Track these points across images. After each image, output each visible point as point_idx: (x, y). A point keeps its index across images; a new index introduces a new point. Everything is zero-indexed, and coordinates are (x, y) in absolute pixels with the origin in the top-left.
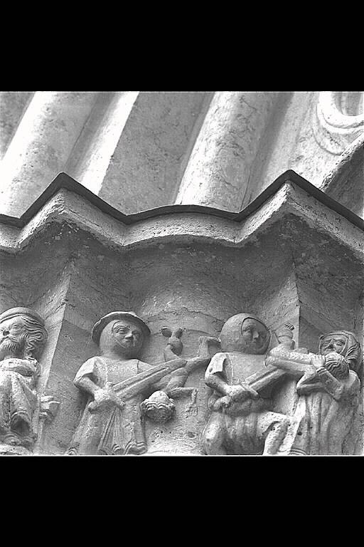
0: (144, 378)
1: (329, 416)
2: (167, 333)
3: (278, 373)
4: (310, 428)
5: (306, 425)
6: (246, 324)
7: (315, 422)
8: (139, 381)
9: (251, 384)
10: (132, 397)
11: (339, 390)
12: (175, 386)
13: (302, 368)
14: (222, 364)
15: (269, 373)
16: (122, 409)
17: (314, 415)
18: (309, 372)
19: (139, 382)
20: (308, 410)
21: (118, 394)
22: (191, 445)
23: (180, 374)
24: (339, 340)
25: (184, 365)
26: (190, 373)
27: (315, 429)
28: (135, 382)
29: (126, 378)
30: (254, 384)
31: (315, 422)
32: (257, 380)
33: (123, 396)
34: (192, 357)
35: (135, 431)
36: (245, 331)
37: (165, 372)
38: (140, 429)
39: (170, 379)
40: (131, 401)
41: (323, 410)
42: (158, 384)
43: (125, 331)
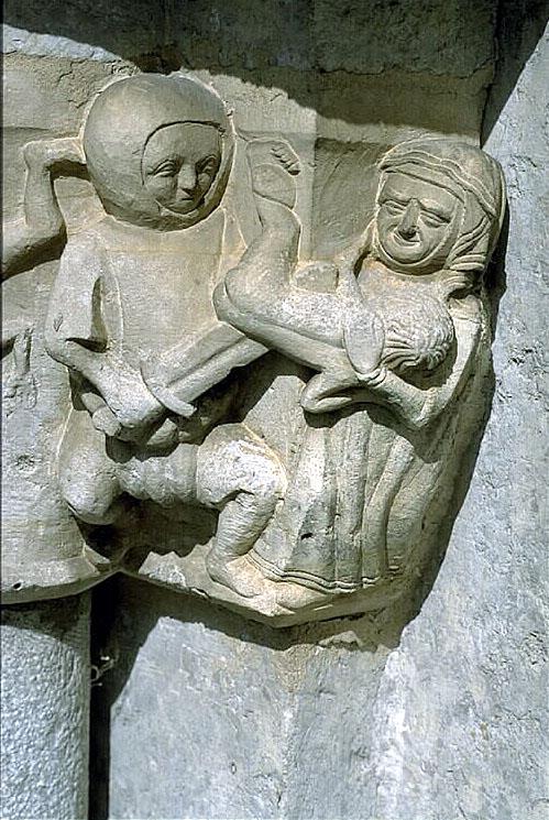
1: (389, 477)
3: (249, 351)
4: (333, 513)
5: (324, 516)
6: (157, 152)
7: (348, 505)
9: (173, 382)
11: (420, 417)
13: (312, 353)
14: (87, 300)
15: (221, 351)
17: (345, 483)
18: (336, 371)
20: (330, 472)
24: (431, 210)
27: (347, 522)
30: (183, 384)
31: (348, 505)
32: (191, 371)
36: (155, 172)
41: (370, 469)
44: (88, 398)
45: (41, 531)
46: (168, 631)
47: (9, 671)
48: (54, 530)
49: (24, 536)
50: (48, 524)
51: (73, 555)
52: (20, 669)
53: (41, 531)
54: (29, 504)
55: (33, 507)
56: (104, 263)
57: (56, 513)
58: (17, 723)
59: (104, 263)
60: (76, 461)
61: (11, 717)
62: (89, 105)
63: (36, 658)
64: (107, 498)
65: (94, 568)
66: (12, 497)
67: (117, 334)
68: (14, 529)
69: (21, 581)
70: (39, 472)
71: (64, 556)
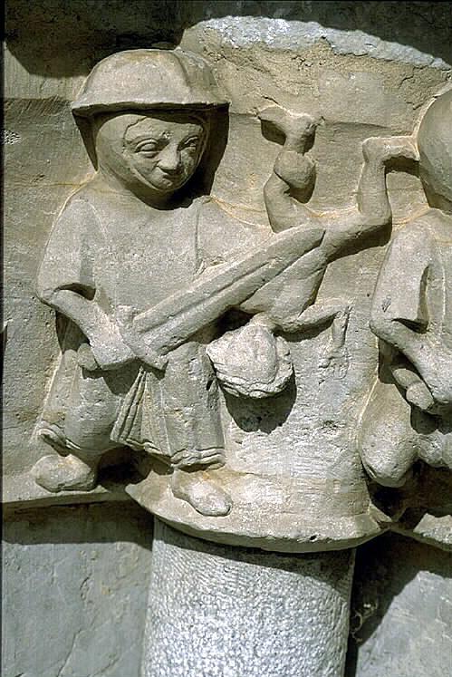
0: (213, 294)
2: (273, 132)
8: (198, 303)
10: (187, 341)
12: (293, 312)
14: (415, 285)
16: (160, 373)
19: (201, 307)
21: (149, 339)
22: (328, 455)
23: (305, 273)
25: (317, 244)
26: (331, 259)
28: (189, 307)
29: (168, 290)
33: (162, 343)
34: (339, 203)
35: (194, 425)
37: (268, 272)
38: (205, 419)
39: (279, 289)
40: (183, 349)
42: (248, 305)
43: (160, 145)
44: (401, 374)
45: (337, 489)
46: (426, 584)
47: (292, 613)
48: (347, 489)
49: (322, 492)
50: (343, 484)
51: (358, 512)
52: (300, 611)
53: (337, 489)
54: (329, 464)
55: (332, 468)
56: (433, 252)
57: (351, 474)
58: (293, 660)
59: (433, 252)
60: (381, 428)
61: (289, 654)
62: (425, 108)
63: (314, 602)
64: (405, 465)
65: (377, 526)
66: (316, 458)
67: (439, 317)
68: (313, 486)
69: (316, 533)
70: (341, 436)
71: (353, 512)
